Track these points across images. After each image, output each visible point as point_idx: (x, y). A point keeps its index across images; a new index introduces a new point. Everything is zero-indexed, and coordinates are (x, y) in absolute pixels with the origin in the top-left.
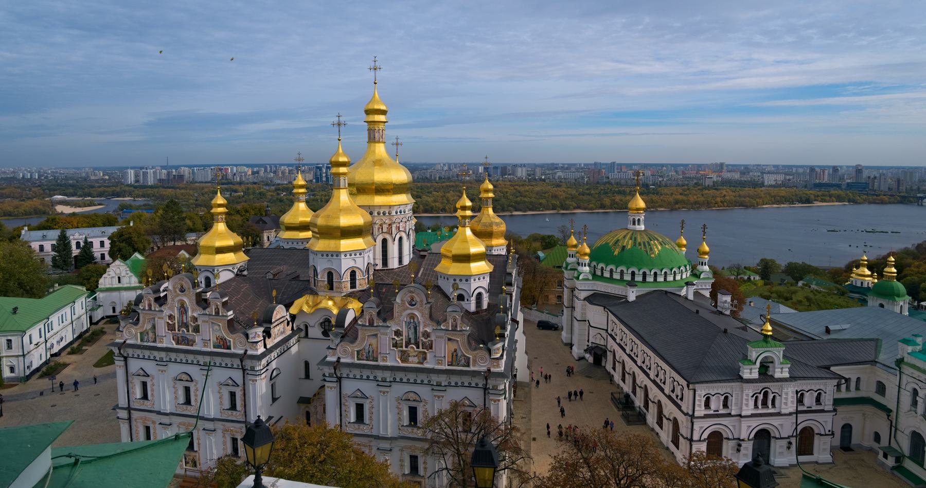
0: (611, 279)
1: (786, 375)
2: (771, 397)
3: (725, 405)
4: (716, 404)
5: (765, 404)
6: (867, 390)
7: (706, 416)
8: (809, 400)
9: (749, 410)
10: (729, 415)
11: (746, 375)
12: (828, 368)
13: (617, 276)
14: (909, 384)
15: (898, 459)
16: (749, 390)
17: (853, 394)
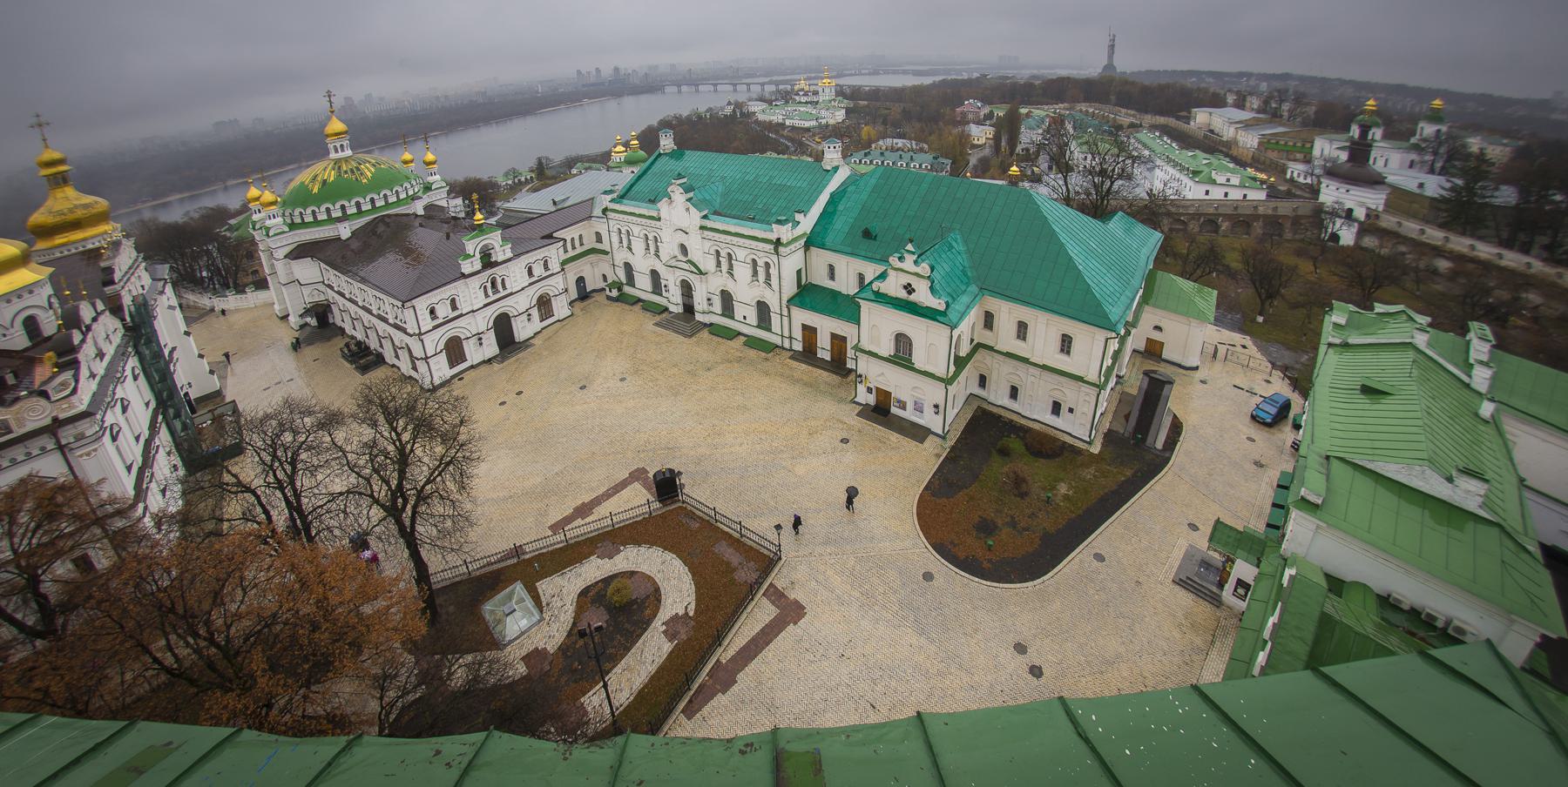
0: (317, 223)
1: (509, 254)
2: (499, 281)
3: (454, 308)
4: (444, 311)
5: (496, 291)
6: (590, 243)
7: (435, 328)
8: (538, 271)
9: (481, 300)
10: (461, 315)
11: (467, 268)
12: (550, 236)
13: (322, 217)
14: (614, 226)
15: (620, 289)
16: (475, 283)
17: (579, 250)
